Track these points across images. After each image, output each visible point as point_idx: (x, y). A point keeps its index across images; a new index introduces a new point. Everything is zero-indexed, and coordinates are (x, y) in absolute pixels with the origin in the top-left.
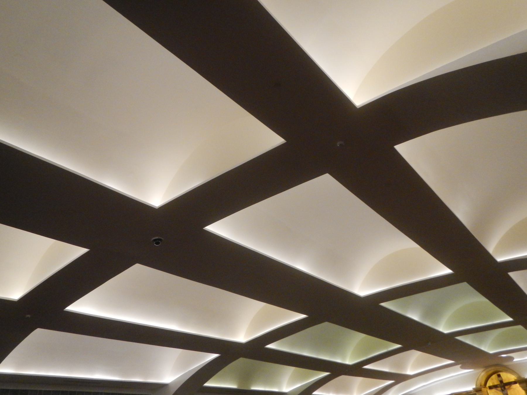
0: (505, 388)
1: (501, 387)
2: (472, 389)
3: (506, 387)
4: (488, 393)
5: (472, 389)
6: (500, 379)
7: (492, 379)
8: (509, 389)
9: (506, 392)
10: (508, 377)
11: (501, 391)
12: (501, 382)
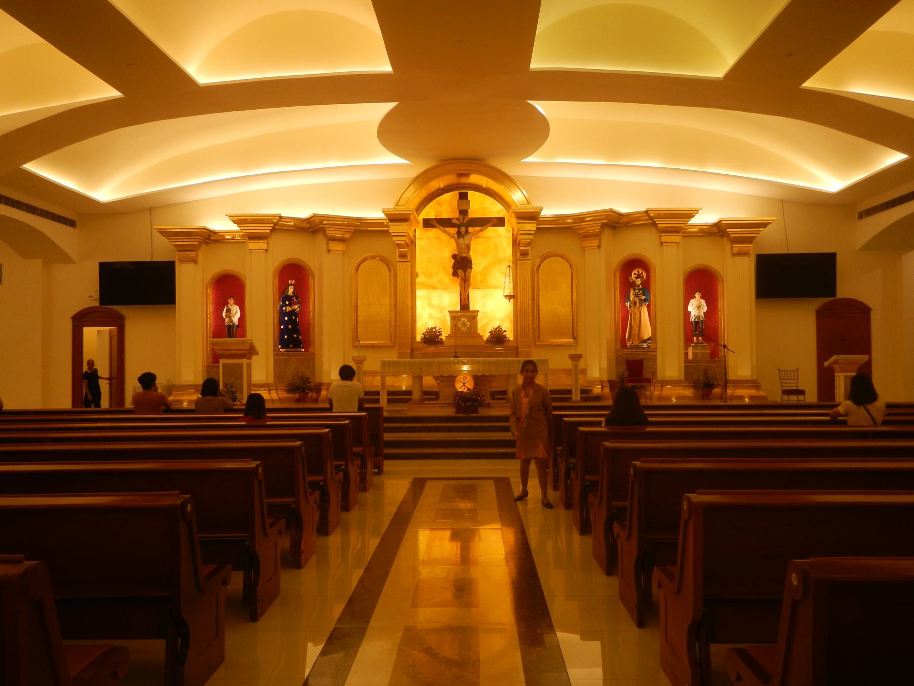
0: (467, 232)
2: (382, 215)
3: (470, 229)
4: (415, 236)
5: (382, 215)
6: (464, 208)
7: (440, 204)
9: (467, 242)
11: (456, 236)
12: (464, 212)
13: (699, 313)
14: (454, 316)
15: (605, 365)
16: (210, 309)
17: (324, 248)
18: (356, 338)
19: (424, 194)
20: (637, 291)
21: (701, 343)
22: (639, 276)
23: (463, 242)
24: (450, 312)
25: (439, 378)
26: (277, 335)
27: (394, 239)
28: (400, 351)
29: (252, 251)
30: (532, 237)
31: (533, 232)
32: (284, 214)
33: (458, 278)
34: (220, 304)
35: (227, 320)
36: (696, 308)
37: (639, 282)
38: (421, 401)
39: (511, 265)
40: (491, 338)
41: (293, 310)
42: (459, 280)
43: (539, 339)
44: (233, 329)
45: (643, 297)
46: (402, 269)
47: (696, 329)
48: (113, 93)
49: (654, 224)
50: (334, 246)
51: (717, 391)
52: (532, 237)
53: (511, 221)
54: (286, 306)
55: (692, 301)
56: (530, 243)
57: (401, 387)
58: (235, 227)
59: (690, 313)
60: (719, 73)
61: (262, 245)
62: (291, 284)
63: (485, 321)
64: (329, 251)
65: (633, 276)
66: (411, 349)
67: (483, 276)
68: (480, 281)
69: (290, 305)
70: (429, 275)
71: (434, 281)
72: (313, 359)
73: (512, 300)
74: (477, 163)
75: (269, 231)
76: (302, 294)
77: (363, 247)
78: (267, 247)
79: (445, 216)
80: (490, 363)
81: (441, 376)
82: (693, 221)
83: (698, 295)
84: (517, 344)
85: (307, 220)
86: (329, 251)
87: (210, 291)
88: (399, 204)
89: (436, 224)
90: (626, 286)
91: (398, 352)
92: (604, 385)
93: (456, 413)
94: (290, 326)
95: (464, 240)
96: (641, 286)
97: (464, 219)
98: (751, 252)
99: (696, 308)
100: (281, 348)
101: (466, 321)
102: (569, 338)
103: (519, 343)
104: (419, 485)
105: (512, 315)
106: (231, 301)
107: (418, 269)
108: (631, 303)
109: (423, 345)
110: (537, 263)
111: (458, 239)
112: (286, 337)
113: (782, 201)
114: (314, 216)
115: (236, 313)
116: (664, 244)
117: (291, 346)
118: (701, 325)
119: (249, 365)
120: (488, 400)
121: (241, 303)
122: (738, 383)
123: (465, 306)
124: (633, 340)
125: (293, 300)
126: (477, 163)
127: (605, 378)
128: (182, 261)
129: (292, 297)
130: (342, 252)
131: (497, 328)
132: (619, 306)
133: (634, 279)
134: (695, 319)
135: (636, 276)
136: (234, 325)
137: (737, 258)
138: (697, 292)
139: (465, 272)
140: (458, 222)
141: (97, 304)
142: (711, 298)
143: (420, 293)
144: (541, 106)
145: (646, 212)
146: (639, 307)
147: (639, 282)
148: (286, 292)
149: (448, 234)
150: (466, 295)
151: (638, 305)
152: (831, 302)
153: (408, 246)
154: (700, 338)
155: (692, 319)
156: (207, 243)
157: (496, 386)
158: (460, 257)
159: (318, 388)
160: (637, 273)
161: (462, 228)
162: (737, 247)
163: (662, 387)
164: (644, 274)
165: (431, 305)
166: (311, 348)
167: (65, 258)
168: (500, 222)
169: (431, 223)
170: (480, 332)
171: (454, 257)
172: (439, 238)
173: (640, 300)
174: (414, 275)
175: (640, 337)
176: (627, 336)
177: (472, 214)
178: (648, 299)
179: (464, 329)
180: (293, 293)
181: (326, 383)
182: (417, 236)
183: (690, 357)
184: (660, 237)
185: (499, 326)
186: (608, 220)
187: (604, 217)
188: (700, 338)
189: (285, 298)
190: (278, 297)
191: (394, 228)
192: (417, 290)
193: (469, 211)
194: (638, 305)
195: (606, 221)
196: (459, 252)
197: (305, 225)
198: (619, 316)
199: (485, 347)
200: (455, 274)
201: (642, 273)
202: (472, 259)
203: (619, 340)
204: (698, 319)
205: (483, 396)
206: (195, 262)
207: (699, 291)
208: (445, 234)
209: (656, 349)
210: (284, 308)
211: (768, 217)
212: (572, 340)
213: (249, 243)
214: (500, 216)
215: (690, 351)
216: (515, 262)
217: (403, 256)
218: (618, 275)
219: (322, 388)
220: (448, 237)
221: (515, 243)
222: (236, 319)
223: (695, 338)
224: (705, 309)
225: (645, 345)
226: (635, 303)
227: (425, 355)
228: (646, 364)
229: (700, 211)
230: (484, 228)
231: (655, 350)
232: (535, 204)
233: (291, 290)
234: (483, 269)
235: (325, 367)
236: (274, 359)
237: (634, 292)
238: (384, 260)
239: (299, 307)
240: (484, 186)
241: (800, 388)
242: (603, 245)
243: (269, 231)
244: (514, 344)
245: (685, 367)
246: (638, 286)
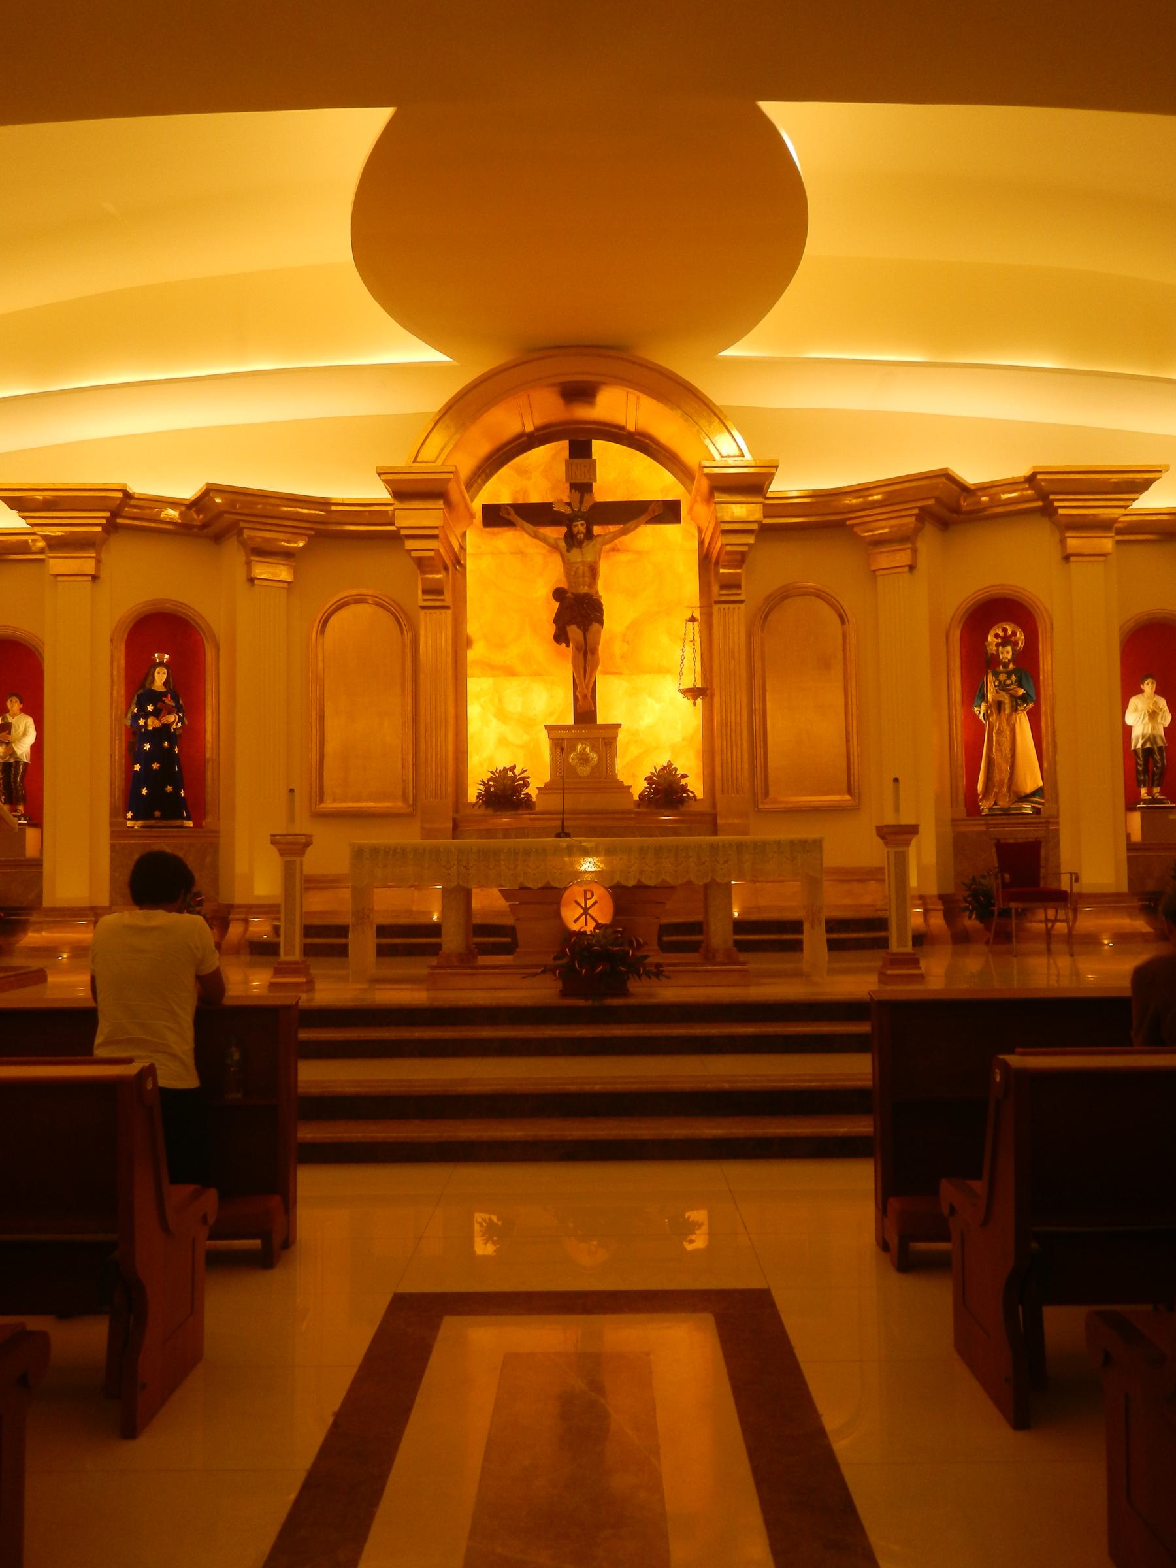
0: (589, 535)
4: (463, 548)
9: (589, 558)
11: (562, 544)
12: (582, 488)
13: (1154, 728)
14: (560, 741)
17: (240, 574)
20: (1003, 677)
21: (1161, 802)
22: (1006, 641)
23: (579, 559)
24: (549, 728)
25: (517, 895)
26: (120, 782)
27: (410, 544)
28: (427, 826)
29: (59, 578)
31: (755, 526)
33: (568, 646)
38: (467, 959)
39: (697, 615)
40: (650, 793)
41: (163, 724)
42: (570, 651)
43: (766, 794)
44: (16, 774)
45: (1021, 692)
47: (1146, 771)
49: (1048, 511)
50: (263, 570)
52: (751, 540)
54: (146, 715)
55: (1135, 701)
57: (430, 914)
62: (161, 664)
63: (634, 751)
66: (454, 821)
67: (628, 642)
68: (622, 657)
69: (157, 714)
70: (499, 644)
72: (214, 847)
73: (699, 701)
78: (97, 568)
79: (535, 498)
80: (658, 850)
81: (523, 888)
83: (1148, 687)
84: (714, 805)
86: (251, 580)
88: (418, 460)
89: (514, 517)
91: (422, 828)
92: (931, 907)
93: (564, 994)
94: (155, 766)
95: (583, 554)
96: (1011, 666)
97: (581, 502)
100: (132, 819)
101: (588, 749)
102: (839, 793)
103: (718, 806)
105: (700, 736)
106: (14, 705)
107: (473, 628)
108: (989, 707)
109: (482, 811)
111: (568, 551)
112: (145, 791)
114: (210, 490)
115: (25, 734)
116: (1072, 559)
117: (157, 814)
118: (1158, 757)
120: (656, 957)
121: (35, 709)
123: (585, 712)
124: (997, 794)
125: (163, 702)
127: (932, 890)
129: (163, 694)
130: (286, 585)
131: (664, 768)
134: (1143, 745)
135: (1000, 640)
136: (17, 763)
138: (1147, 677)
139: (585, 631)
140: (568, 510)
143: (477, 685)
145: (1031, 479)
146: (1010, 715)
147: (1007, 654)
148: (148, 682)
149: (544, 540)
150: (587, 687)
151: (1008, 711)
153: (446, 568)
154: (1156, 790)
155: (1137, 742)
157: (677, 911)
158: (572, 593)
160: (1001, 634)
161: (579, 523)
164: (1020, 636)
165: (502, 715)
166: (209, 819)
168: (669, 512)
169: (503, 514)
170: (623, 776)
171: (559, 594)
172: (522, 553)
173: (1013, 698)
174: (460, 643)
175: (1013, 788)
176: (980, 787)
178: (1033, 694)
179: (583, 771)
181: (240, 906)
183: (1137, 837)
184: (1063, 541)
185: (670, 764)
186: (938, 500)
188: (1156, 790)
190: (123, 692)
192: (468, 679)
194: (1008, 711)
196: (569, 582)
199: (636, 813)
200: (560, 637)
201: (1014, 634)
202: (603, 601)
203: (961, 797)
204: (1152, 744)
205: (640, 946)
208: (536, 541)
209: (1057, 817)
210: (141, 722)
212: (848, 797)
213: (51, 560)
214: (670, 497)
215: (1136, 819)
219: (231, 917)
221: (707, 562)
222: (23, 748)
223: (1143, 791)
224: (1167, 719)
226: (999, 705)
227: (489, 833)
230: (628, 525)
231: (1054, 819)
233: (160, 678)
234: (628, 628)
235: (241, 866)
236: (112, 847)
237: (997, 678)
239: (181, 720)
240: (631, 427)
242: (923, 563)
243: (99, 529)
244: (705, 808)
245: (1129, 859)
246: (1006, 665)
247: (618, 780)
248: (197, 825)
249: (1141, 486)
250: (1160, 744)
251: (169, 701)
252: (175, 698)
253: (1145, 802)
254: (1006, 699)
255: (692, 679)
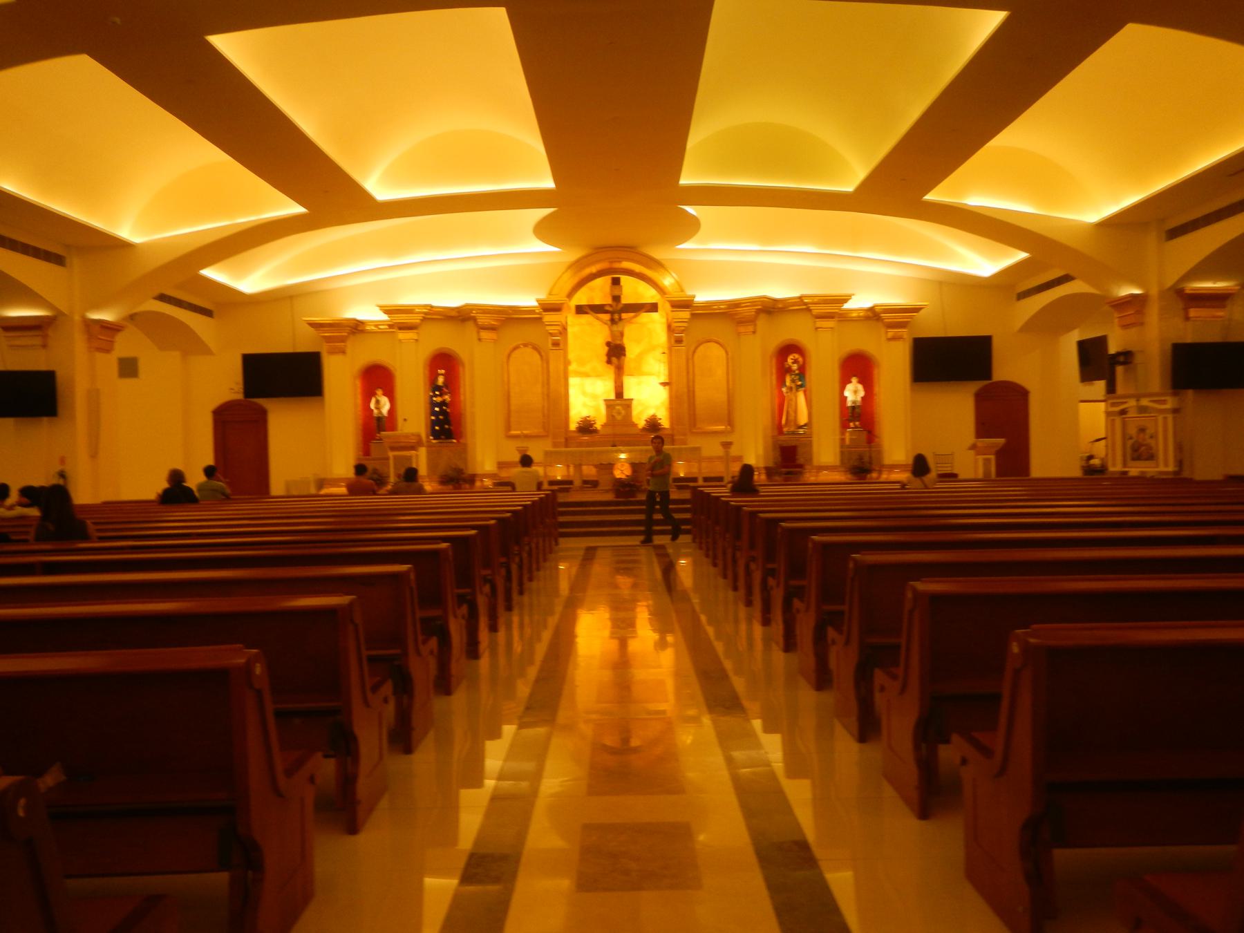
0: (620, 319)
1: (612, 313)
2: (536, 304)
3: (624, 316)
4: (567, 323)
5: (536, 304)
6: (616, 293)
8: (630, 321)
9: (620, 329)
10: (634, 290)
11: (609, 323)
12: (616, 299)
13: (856, 398)
14: (609, 404)
15: (761, 451)
16: (359, 401)
17: (475, 336)
18: (508, 427)
19: (576, 280)
22: (795, 361)
24: (605, 400)
27: (548, 328)
30: (685, 324)
32: (435, 304)
34: (368, 394)
35: (376, 411)
36: (853, 393)
37: (795, 367)
38: (582, 488)
39: (666, 351)
43: (695, 425)
45: (800, 383)
46: (553, 355)
48: (298, 209)
49: (809, 310)
50: (484, 334)
51: (874, 475)
52: (685, 324)
53: (664, 307)
54: (436, 396)
56: (683, 331)
57: (556, 477)
58: (385, 317)
59: (846, 398)
60: (850, 188)
61: (410, 335)
64: (480, 340)
65: (790, 361)
69: (441, 395)
71: (587, 368)
74: (630, 251)
75: (418, 321)
76: (452, 384)
77: (513, 336)
79: (597, 302)
81: (601, 464)
82: (846, 306)
83: (854, 380)
85: (458, 309)
86: (480, 340)
87: (358, 383)
89: (589, 311)
90: (783, 371)
97: (617, 305)
98: (905, 336)
99: (853, 393)
100: (434, 439)
104: (590, 554)
106: (379, 392)
107: (571, 356)
110: (692, 348)
113: (941, 283)
114: (467, 305)
115: (385, 405)
117: (443, 437)
119: (417, 455)
121: (390, 394)
122: (892, 467)
123: (619, 394)
126: (630, 251)
128: (332, 352)
132: (776, 392)
133: (790, 364)
137: (893, 343)
141: (240, 396)
142: (867, 382)
143: (574, 382)
144: (690, 209)
145: (800, 298)
147: (795, 367)
151: (794, 390)
152: (986, 386)
154: (857, 423)
155: (849, 404)
156: (353, 333)
159: (472, 479)
162: (891, 333)
163: (818, 472)
164: (800, 359)
165: (584, 393)
167: (205, 350)
168: (653, 308)
170: (635, 420)
171: (608, 344)
174: (567, 363)
176: (784, 421)
177: (625, 300)
179: (619, 418)
180: (444, 383)
181: (480, 475)
182: (569, 323)
183: (847, 442)
184: (815, 322)
187: (759, 303)
189: (435, 387)
191: (549, 318)
193: (622, 296)
194: (794, 390)
195: (759, 307)
197: (453, 314)
198: (776, 402)
200: (609, 362)
206: (344, 352)
207: (854, 376)
211: (919, 302)
216: (670, 348)
217: (556, 344)
218: (774, 361)
220: (601, 323)
221: (670, 328)
224: (862, 393)
225: (801, 431)
227: (580, 444)
228: (800, 451)
229: (853, 297)
230: (637, 314)
232: (689, 292)
233: (441, 380)
235: (479, 458)
238: (535, 348)
241: (955, 471)
244: (670, 432)
246: (794, 371)
247: (633, 422)
248: (458, 441)
249: (845, 301)
250: (858, 404)
251: (445, 390)
252: (447, 388)
253: (852, 428)
254: (793, 385)
255: (664, 379)
